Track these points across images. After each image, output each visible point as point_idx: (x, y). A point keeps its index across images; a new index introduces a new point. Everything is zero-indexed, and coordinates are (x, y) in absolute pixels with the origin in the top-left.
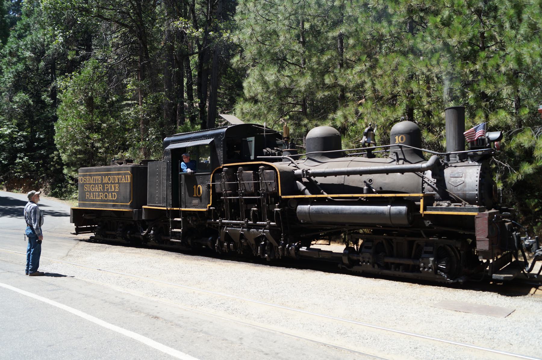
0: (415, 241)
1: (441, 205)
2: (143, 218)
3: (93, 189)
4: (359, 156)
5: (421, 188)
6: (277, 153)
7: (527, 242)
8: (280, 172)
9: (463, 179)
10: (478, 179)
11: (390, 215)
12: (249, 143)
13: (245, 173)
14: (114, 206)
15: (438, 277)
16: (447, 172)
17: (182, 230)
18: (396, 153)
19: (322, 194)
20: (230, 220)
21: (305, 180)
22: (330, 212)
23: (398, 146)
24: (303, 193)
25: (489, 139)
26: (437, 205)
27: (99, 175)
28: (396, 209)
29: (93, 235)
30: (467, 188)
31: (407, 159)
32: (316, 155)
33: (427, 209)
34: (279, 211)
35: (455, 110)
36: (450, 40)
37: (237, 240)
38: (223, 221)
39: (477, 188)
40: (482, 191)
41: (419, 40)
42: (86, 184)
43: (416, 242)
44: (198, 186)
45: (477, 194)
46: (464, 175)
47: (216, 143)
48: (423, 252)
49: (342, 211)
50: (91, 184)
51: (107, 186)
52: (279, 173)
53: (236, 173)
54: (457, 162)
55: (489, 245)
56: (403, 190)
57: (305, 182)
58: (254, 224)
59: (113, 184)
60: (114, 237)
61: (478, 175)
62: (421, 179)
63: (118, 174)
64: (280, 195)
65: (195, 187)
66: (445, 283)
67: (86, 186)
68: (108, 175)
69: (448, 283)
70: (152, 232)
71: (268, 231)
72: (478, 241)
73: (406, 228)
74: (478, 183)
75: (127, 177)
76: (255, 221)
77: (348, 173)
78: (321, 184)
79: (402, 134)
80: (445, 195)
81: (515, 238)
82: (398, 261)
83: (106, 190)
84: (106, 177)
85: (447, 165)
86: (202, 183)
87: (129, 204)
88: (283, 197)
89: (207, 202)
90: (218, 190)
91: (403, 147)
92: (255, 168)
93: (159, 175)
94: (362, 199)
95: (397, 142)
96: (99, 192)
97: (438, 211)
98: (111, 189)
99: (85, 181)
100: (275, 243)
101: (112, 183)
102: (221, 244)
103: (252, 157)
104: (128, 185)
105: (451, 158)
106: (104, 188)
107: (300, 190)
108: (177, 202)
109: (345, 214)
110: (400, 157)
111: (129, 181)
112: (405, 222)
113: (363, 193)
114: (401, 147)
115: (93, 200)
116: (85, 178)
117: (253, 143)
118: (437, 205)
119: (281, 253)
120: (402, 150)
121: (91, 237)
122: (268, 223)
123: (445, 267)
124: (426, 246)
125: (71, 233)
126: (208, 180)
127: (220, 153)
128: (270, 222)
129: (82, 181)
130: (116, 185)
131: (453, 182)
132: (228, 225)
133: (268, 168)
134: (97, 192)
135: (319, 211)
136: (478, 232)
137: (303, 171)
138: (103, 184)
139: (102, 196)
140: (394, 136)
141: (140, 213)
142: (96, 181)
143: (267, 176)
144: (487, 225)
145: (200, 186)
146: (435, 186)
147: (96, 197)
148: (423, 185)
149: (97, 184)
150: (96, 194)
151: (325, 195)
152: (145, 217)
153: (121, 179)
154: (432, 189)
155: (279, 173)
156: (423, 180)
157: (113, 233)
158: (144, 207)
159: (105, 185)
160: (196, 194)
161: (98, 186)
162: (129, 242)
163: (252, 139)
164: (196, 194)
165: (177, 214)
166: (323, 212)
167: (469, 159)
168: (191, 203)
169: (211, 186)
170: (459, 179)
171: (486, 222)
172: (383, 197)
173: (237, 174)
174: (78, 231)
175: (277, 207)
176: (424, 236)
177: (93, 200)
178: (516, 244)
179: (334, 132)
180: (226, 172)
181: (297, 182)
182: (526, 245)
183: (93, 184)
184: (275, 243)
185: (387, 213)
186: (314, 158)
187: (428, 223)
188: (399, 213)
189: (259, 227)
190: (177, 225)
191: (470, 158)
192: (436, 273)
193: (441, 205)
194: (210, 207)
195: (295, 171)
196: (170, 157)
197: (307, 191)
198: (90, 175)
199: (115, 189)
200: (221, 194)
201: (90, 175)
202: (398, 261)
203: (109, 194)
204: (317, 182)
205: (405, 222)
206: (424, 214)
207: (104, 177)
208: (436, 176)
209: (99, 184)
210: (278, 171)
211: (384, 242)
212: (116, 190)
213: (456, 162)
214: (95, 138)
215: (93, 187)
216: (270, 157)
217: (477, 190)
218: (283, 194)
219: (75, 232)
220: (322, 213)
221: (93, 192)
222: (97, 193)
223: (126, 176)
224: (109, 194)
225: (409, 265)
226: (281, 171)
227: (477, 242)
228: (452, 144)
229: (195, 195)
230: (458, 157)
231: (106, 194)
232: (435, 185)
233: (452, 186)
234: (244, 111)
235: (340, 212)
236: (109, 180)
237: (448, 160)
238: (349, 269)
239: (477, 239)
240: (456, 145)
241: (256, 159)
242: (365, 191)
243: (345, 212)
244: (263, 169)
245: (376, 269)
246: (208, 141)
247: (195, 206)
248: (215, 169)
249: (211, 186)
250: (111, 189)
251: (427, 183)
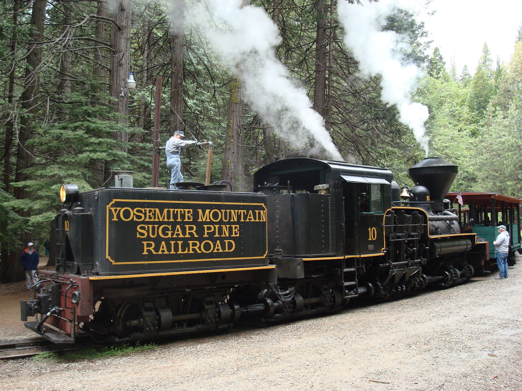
42: (143, 222)
50: (160, 223)
59: (225, 224)
67: (142, 228)
75: (259, 213)
83: (206, 236)
84: (207, 211)
101: (221, 222)
116: (138, 211)
130: (233, 226)
145: (374, 228)
149: (179, 223)
159: (206, 226)
160: (371, 238)
164: (371, 238)
207: (200, 211)
212: (234, 235)
221: (167, 241)
222: (180, 243)
223: (257, 211)
224: (214, 240)
236: (216, 215)
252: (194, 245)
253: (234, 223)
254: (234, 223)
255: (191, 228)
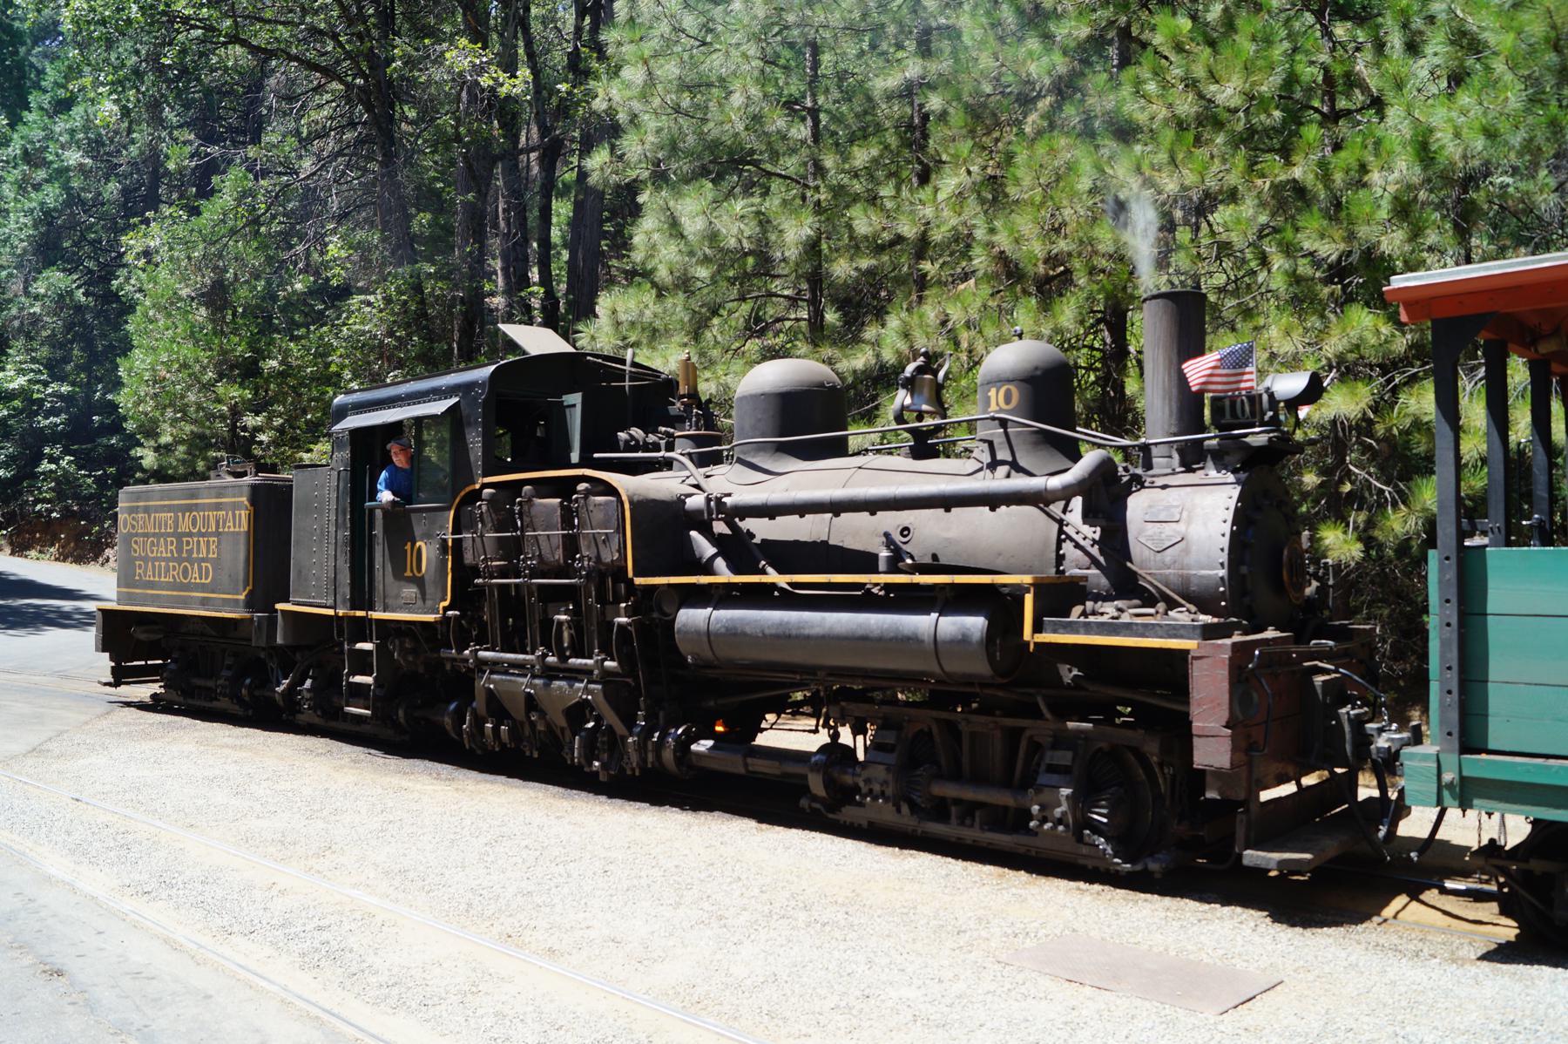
0: (1023, 729)
1: (1102, 614)
2: (279, 641)
3: (152, 552)
4: (891, 454)
5: (1053, 555)
6: (663, 442)
7: (1382, 742)
8: (631, 502)
9: (1181, 527)
10: (1227, 528)
11: (937, 645)
12: (567, 411)
13: (541, 504)
14: (204, 603)
15: (1085, 850)
16: (1137, 504)
17: (376, 679)
18: (991, 444)
19: (763, 572)
20: (502, 651)
21: (720, 527)
22: (767, 632)
23: (993, 419)
24: (708, 569)
25: (1271, 396)
26: (1084, 614)
27: (169, 509)
28: (954, 624)
29: (156, 688)
30: (1191, 559)
31: (1022, 463)
32: (761, 448)
33: (1045, 626)
34: (629, 624)
35: (1170, 303)
36: (1213, 88)
37: (518, 711)
38: (482, 654)
39: (1224, 558)
40: (1244, 569)
41: (1126, 91)
42: (137, 535)
43: (1028, 733)
44: (418, 544)
45: (1222, 578)
46: (1185, 514)
47: (465, 410)
48: (1043, 767)
49: (799, 628)
50: (146, 535)
51: (188, 543)
52: (627, 506)
53: (513, 504)
54: (1174, 473)
55: (1234, 750)
56: (998, 564)
57: (720, 535)
58: (563, 666)
59: (203, 535)
60: (211, 694)
61: (1230, 516)
62: (1056, 526)
63: (218, 507)
64: (630, 574)
65: (408, 547)
66: (1108, 870)
67: (136, 542)
68: (190, 508)
69: (1117, 871)
70: (308, 683)
71: (599, 687)
72: (1199, 736)
73: (983, 685)
74: (1225, 542)
76: (563, 658)
77: (836, 508)
78: (763, 541)
79: (1009, 381)
80: (1126, 584)
81: (1347, 728)
82: (970, 794)
83: (184, 555)
85: (1138, 482)
86: (427, 536)
87: (242, 597)
88: (639, 581)
89: (439, 595)
90: (468, 558)
91: (1009, 424)
92: (564, 488)
93: (319, 510)
94: (875, 590)
95: (993, 407)
96: (167, 560)
97: (1077, 632)
98: (198, 552)
99: (133, 527)
100: (620, 728)
102: (478, 722)
103: (575, 457)
104: (242, 540)
105: (1155, 460)
106: (179, 550)
107: (701, 558)
108: (362, 595)
109: (808, 637)
110: (1000, 457)
111: (245, 527)
112: (980, 667)
113: (877, 572)
114: (1003, 423)
115: (152, 585)
117: (578, 410)
118: (1084, 614)
119: (634, 758)
120: (1006, 434)
121: (154, 696)
122: (597, 661)
123: (1105, 820)
124: (1055, 746)
125: (99, 682)
126: (442, 527)
127: (475, 443)
128: (604, 660)
129: (125, 528)
130: (211, 539)
131: (1151, 538)
132: (495, 666)
133: (601, 488)
134: (164, 559)
135: (735, 628)
136: (1199, 705)
137: (708, 500)
138: (179, 536)
139: (175, 574)
140: (986, 387)
141: (272, 622)
142: (160, 528)
143: (598, 516)
144: (1225, 685)
146: (1095, 551)
147: (160, 576)
148: (1059, 547)
149: (162, 535)
150: (160, 566)
151: (773, 576)
152: (285, 638)
153: (224, 523)
154: (1086, 560)
155: (627, 506)
156: (1061, 532)
157: (210, 684)
158: (279, 606)
159: (185, 539)
160: (412, 571)
161: (166, 542)
162: (250, 712)
163: (575, 399)
165: (361, 629)
166: (748, 630)
167: (1210, 463)
168: (397, 596)
169: (450, 544)
170: (1168, 529)
171: (1223, 673)
172: (917, 585)
173: (517, 508)
174: (120, 676)
175: (622, 612)
176: (1048, 715)
177: (152, 585)
178: (1348, 748)
179: (817, 378)
180: (492, 501)
181: (693, 534)
182: (1379, 749)
183: (154, 535)
184: (620, 728)
185: (926, 638)
186: (754, 460)
187: (1069, 673)
188: (963, 641)
189: (574, 675)
190: (362, 663)
191: (1213, 459)
192: (1080, 838)
193: (1102, 614)
194: (446, 609)
195: (688, 500)
196: (346, 454)
197: (720, 563)
198: (147, 510)
199: (208, 552)
200: (475, 571)
201: (147, 510)
202: (970, 794)
203: (192, 565)
204: (752, 536)
205: (980, 667)
206: (1035, 644)
208: (1095, 516)
209: (169, 535)
210: (624, 498)
211: (935, 730)
212: (211, 556)
213: (1169, 471)
214: (234, 397)
215: (152, 543)
216: (640, 454)
217: (1222, 564)
218: (636, 575)
219: (112, 680)
220: (744, 634)
221: (156, 559)
222: (163, 564)
224: (192, 565)
225: (1006, 808)
226: (636, 498)
227: (1196, 741)
228: (1160, 414)
229: (408, 574)
230: (1176, 456)
231: (186, 567)
232: (1096, 547)
233: (1147, 552)
234: (623, 317)
235: (794, 632)
237: (1148, 466)
238: (830, 816)
239: (1194, 732)
240: (1171, 416)
241: (586, 462)
242: (882, 566)
243: (807, 632)
244: (588, 493)
245: (905, 819)
246: (439, 407)
247: (407, 607)
248: (463, 493)
249: (450, 544)
250: (198, 552)
251: (1072, 540)
252: (174, 568)
253: (212, 534)
254: (212, 534)
255: (172, 543)
